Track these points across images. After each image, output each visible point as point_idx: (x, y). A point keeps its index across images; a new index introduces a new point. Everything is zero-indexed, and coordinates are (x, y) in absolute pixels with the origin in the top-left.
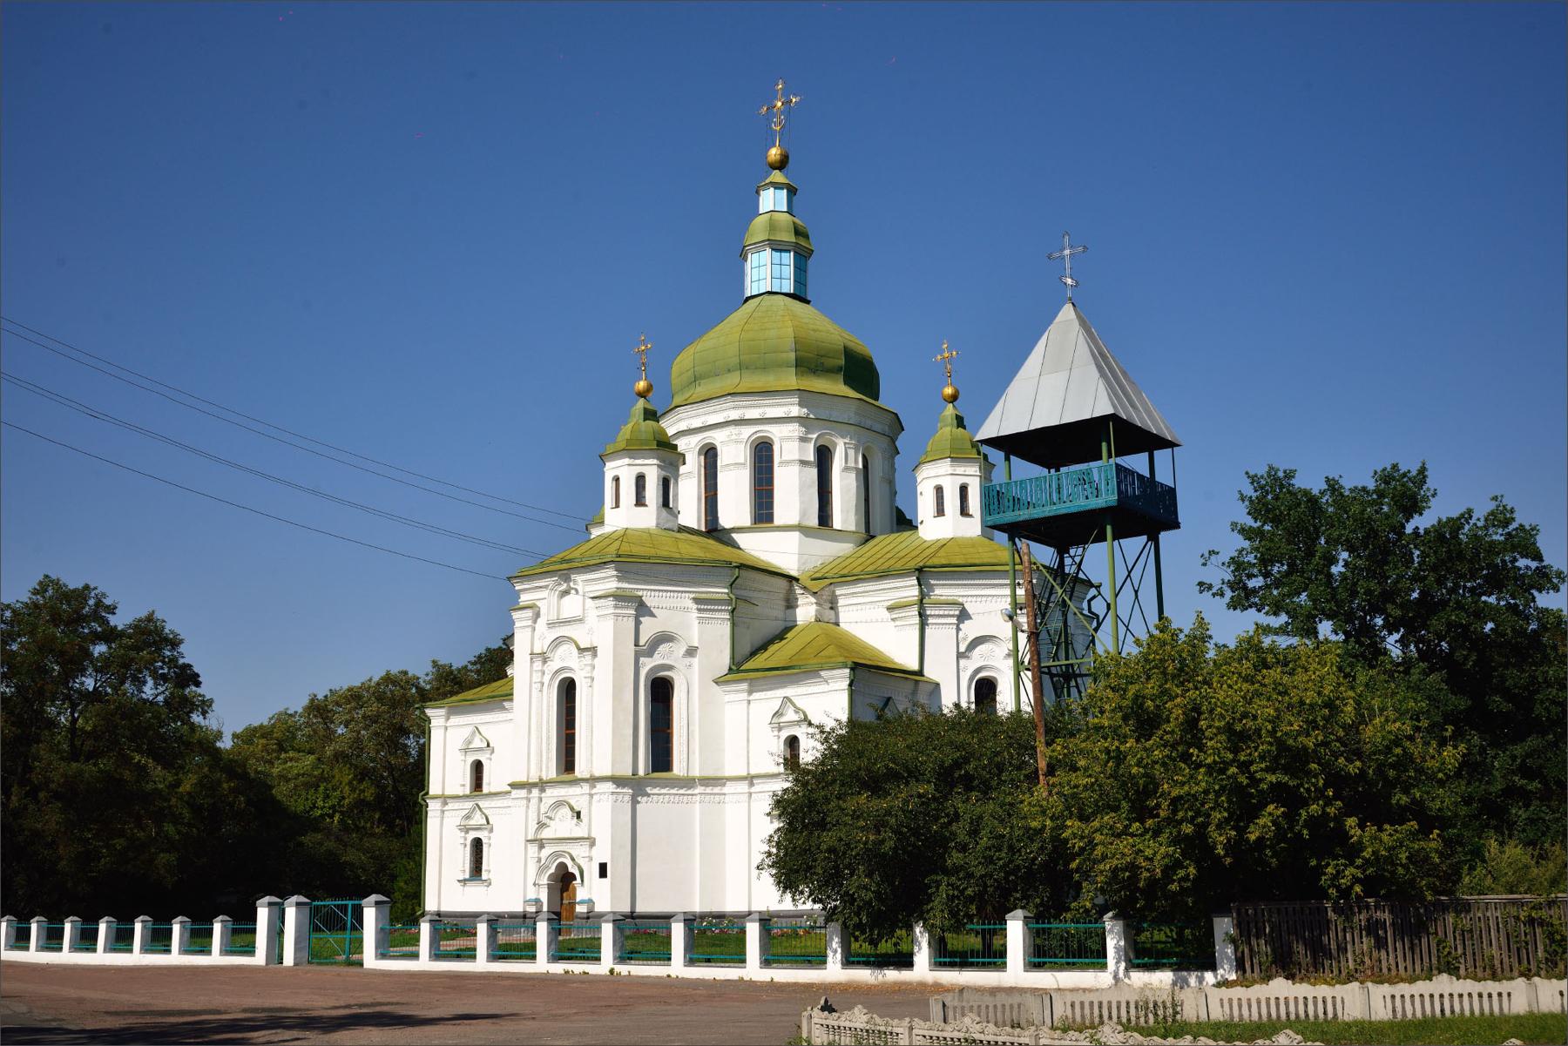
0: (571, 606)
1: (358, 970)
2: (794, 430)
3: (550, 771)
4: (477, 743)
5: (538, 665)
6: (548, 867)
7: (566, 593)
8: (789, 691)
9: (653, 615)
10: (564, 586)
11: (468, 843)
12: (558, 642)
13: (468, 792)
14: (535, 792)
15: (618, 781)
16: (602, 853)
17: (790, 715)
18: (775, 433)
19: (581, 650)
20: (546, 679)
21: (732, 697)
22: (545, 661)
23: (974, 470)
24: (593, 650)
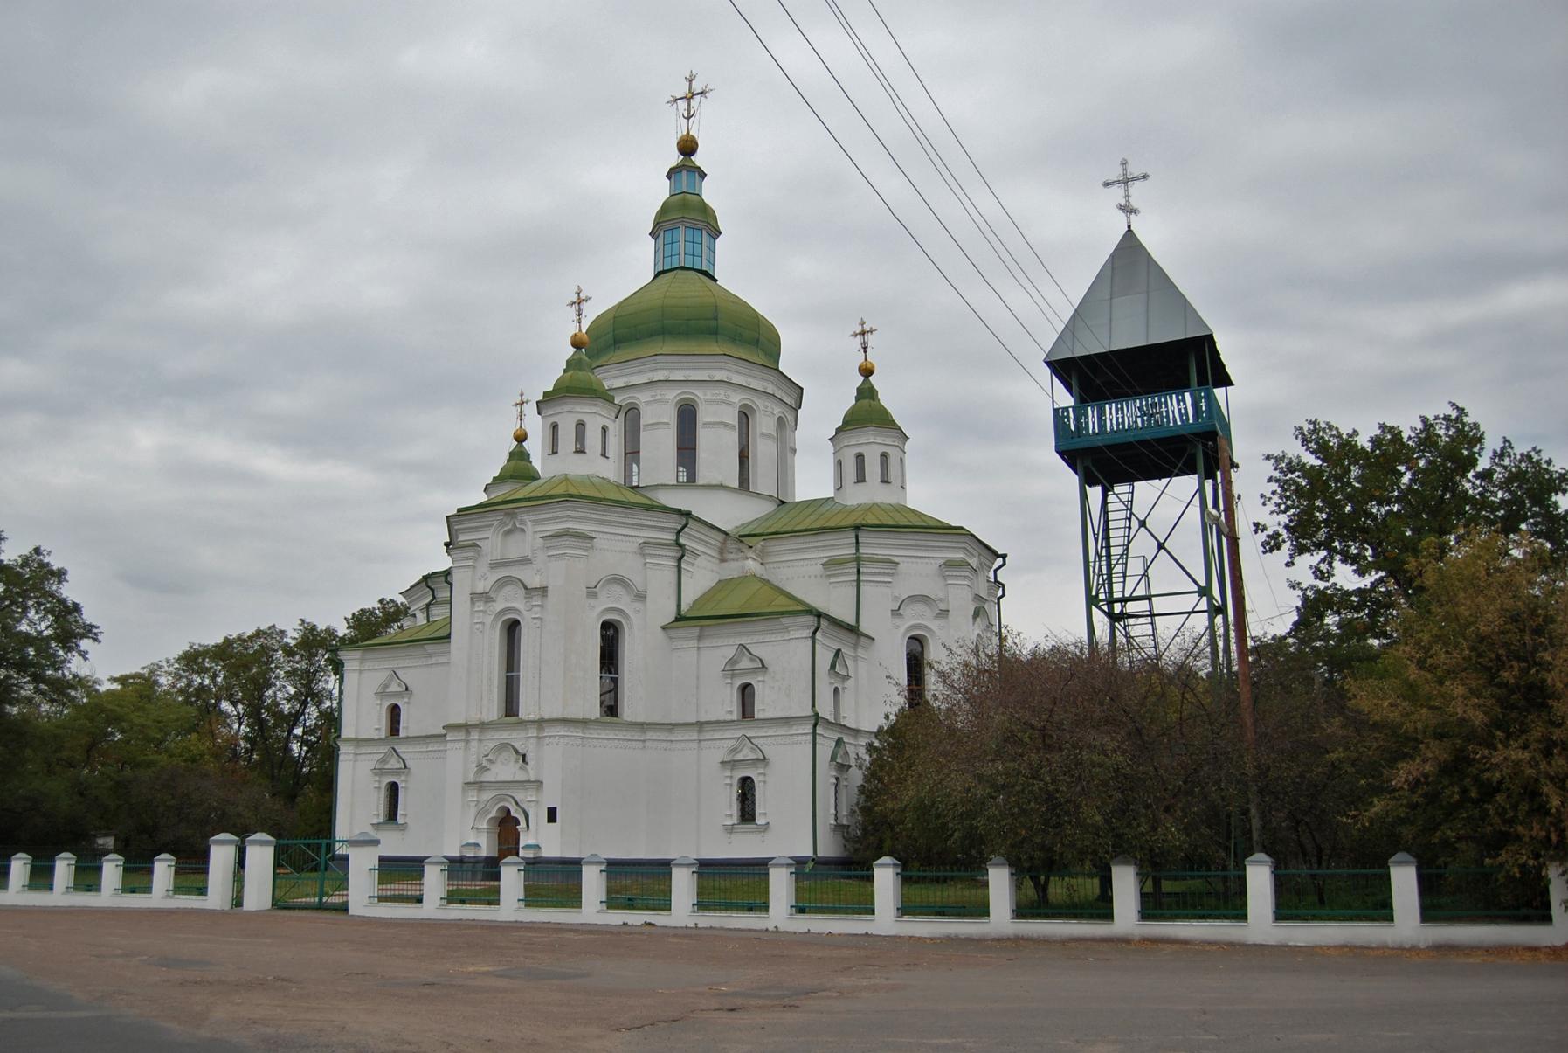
0: (517, 547)
1: (340, 916)
4: (394, 688)
7: (508, 532)
18: (701, 395)
19: (529, 591)
20: (489, 620)
24: (543, 590)
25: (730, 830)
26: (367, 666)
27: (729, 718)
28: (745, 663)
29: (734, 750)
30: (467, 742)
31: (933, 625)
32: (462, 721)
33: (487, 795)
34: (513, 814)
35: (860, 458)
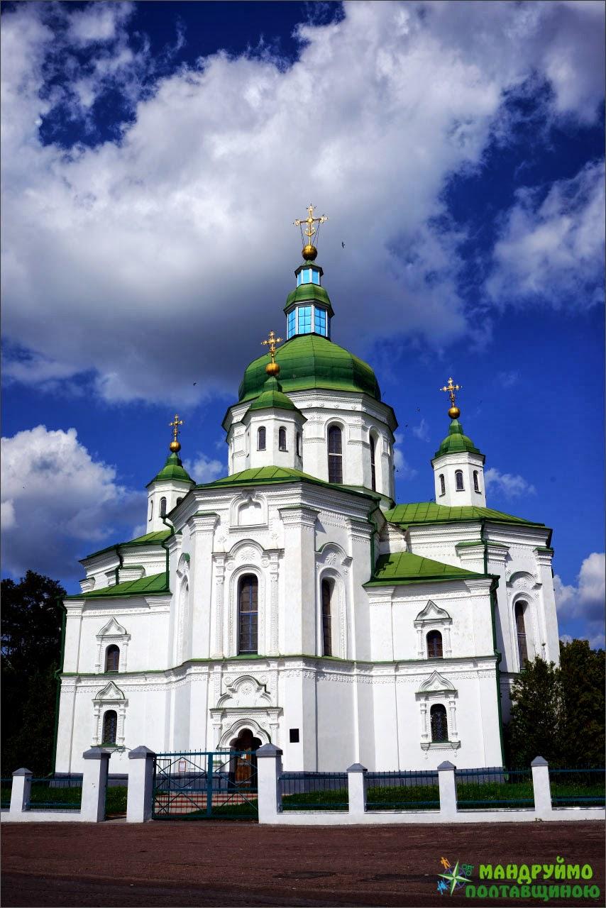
0: (251, 516)
2: (358, 420)
3: (231, 650)
5: (220, 561)
6: (232, 733)
8: (431, 597)
9: (323, 531)
10: (246, 501)
13: (103, 671)
14: (218, 668)
15: (306, 659)
16: (295, 717)
18: (347, 421)
19: (268, 553)
20: (228, 574)
22: (226, 560)
23: (480, 463)
24: (280, 552)
25: (426, 747)
26: (88, 613)
27: (420, 658)
28: (433, 614)
29: (427, 683)
30: (209, 674)
31: (532, 593)
32: (205, 657)
33: (231, 720)
34: (255, 735)
35: (459, 475)
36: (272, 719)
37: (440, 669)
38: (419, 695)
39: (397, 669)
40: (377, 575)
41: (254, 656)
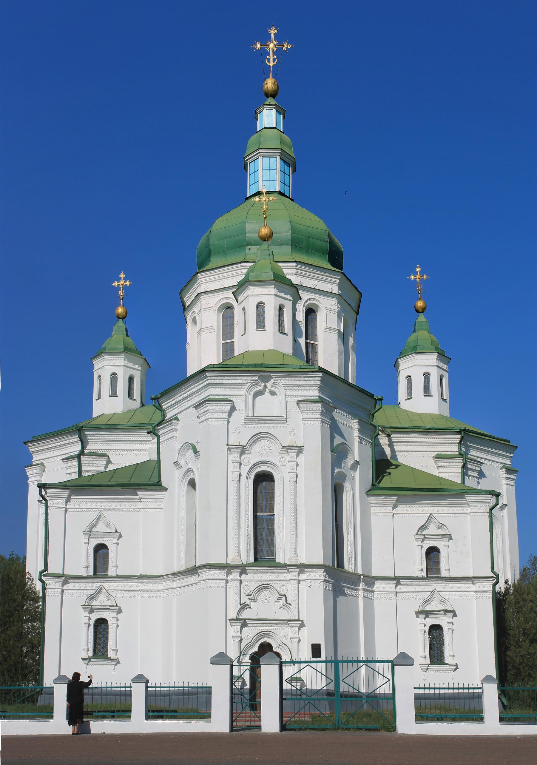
5: (234, 456)
11: (92, 623)
12: (257, 437)
14: (236, 574)
17: (432, 529)
20: (245, 470)
21: (383, 509)
27: (418, 574)
29: (426, 602)
33: (250, 632)
36: (289, 632)
37: (439, 588)
38: (418, 613)
39: (398, 584)
40: (379, 483)
41: (272, 564)
